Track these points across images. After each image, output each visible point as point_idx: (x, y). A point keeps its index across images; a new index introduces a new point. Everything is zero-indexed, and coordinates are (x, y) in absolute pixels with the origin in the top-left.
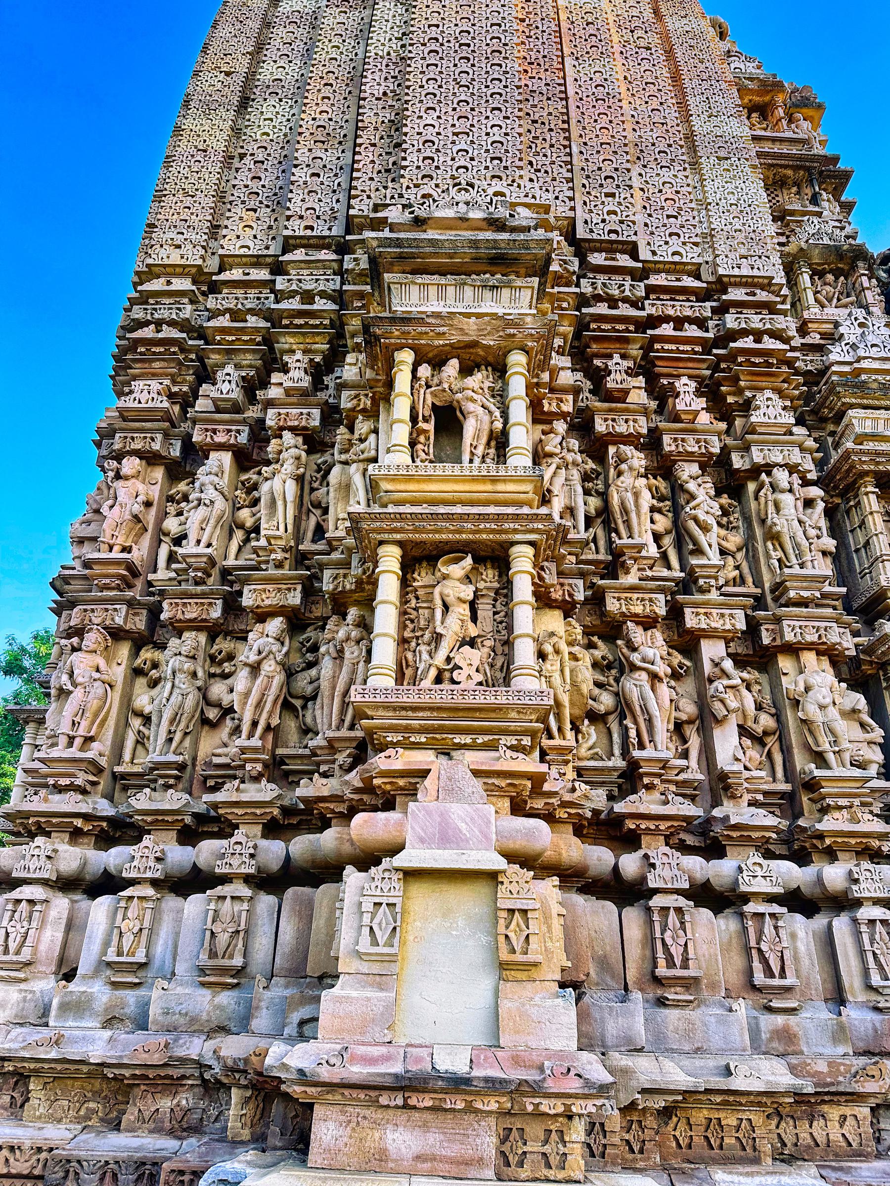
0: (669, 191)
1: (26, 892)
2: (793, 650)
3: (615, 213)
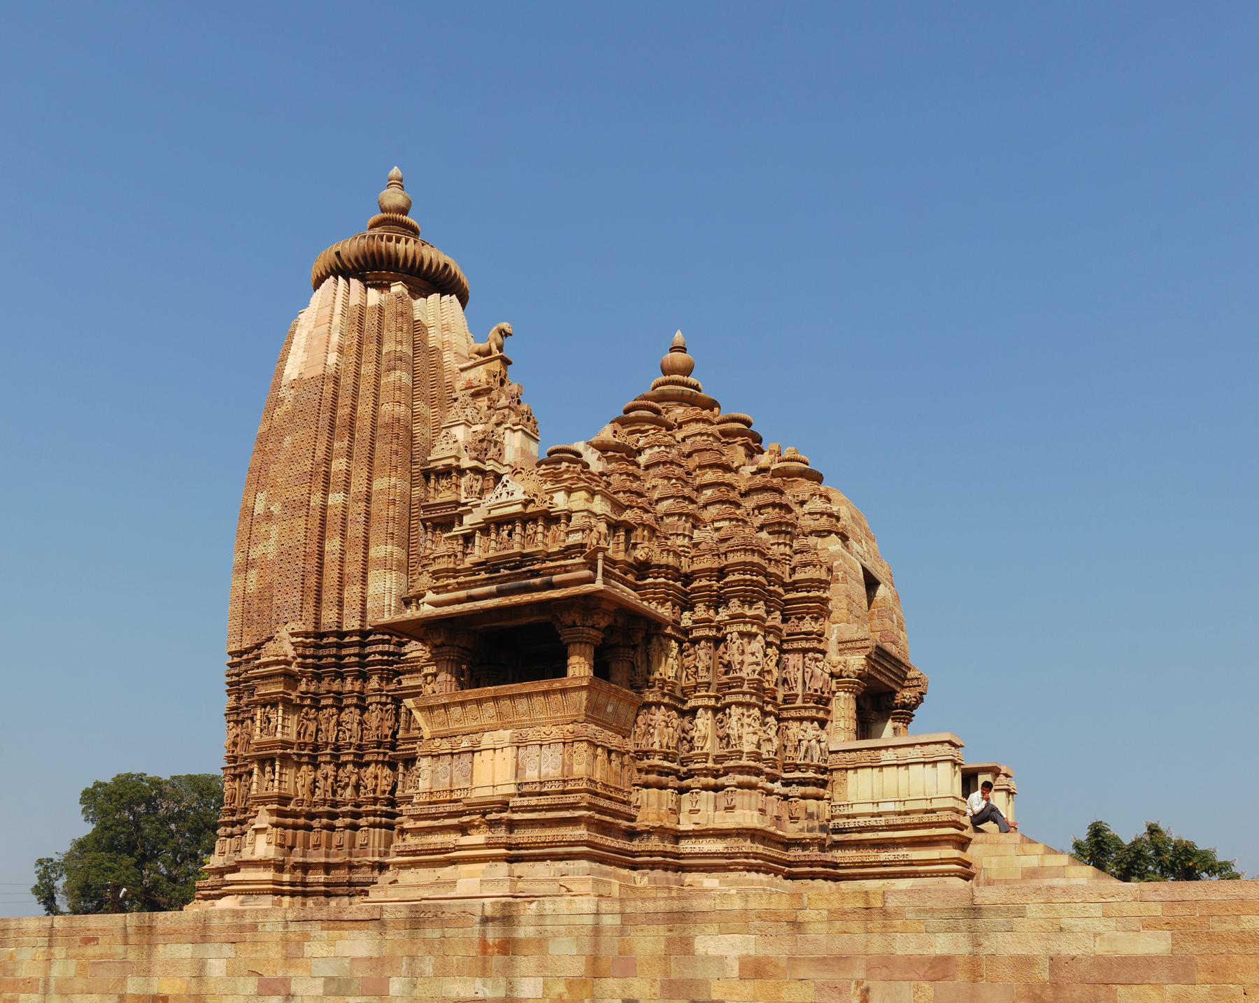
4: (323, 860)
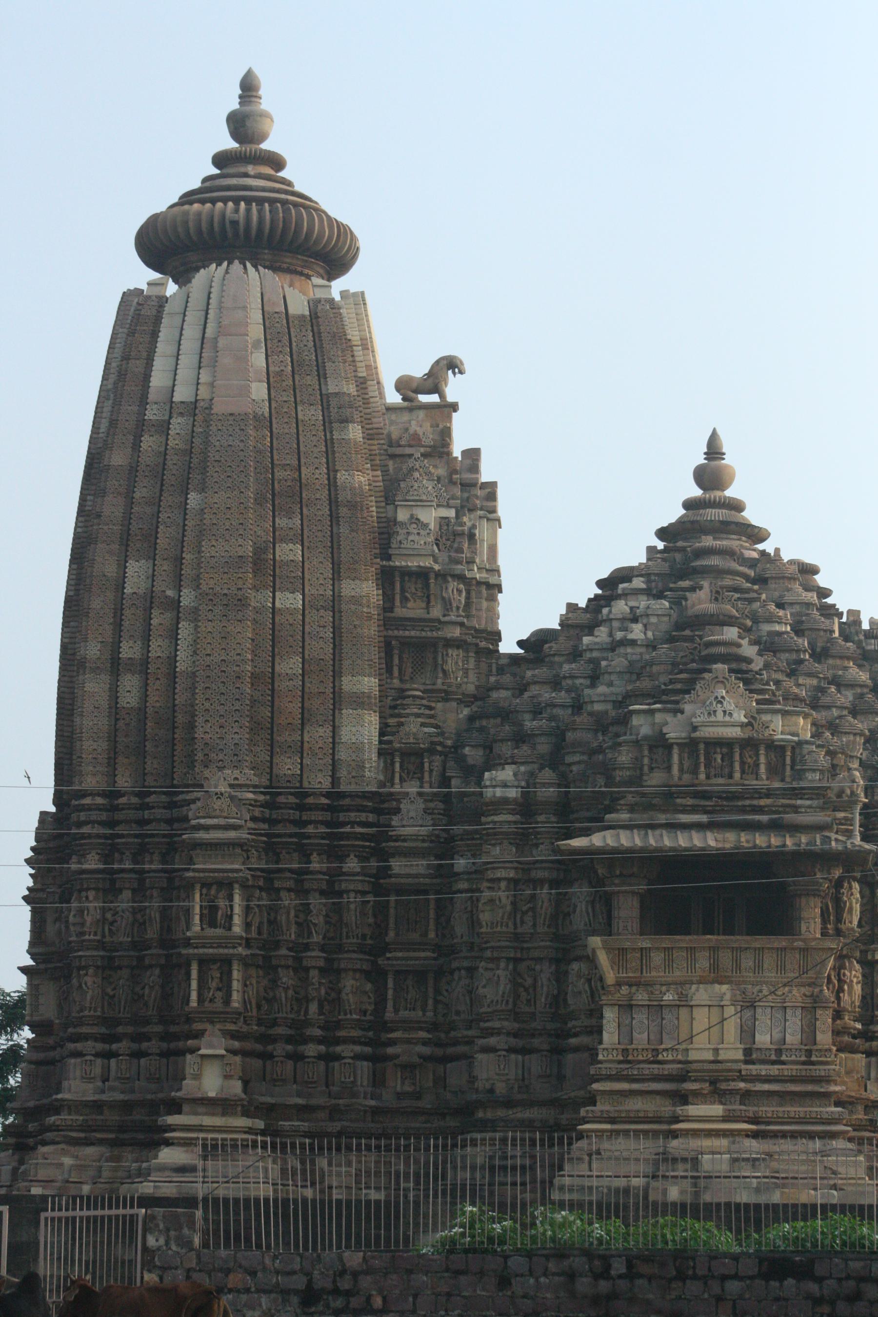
1: (88, 1058)
2: (346, 970)
4: (300, 1101)
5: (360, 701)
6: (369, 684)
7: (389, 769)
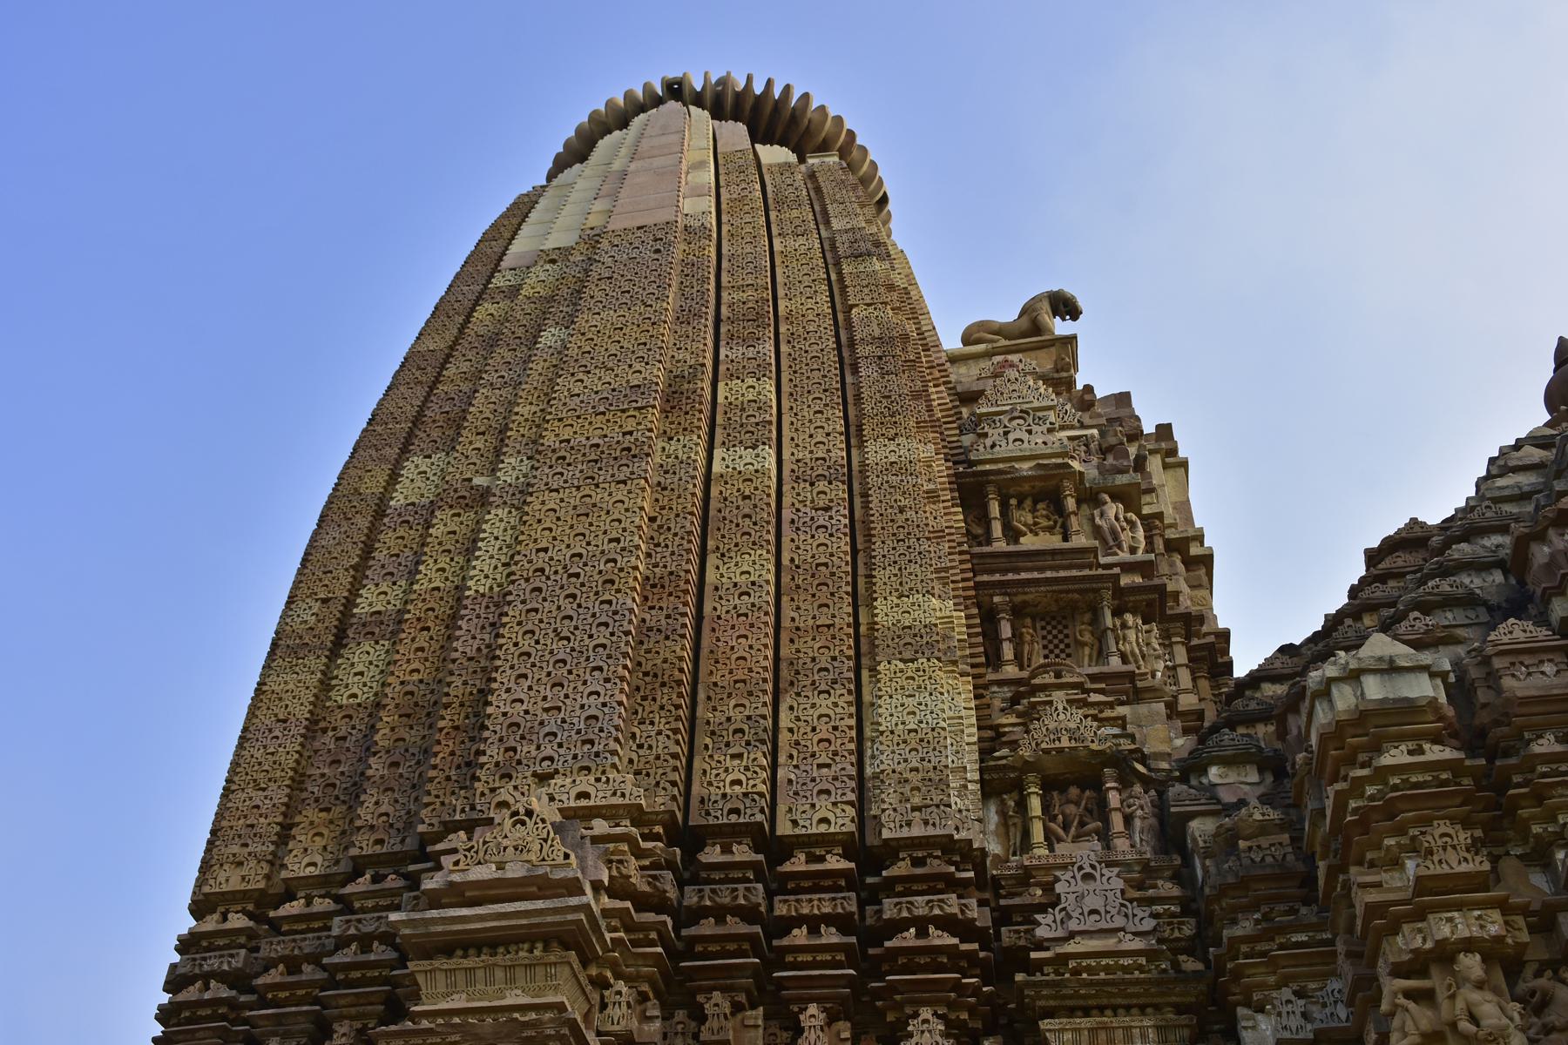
0: (824, 728)
3: (739, 782)
5: (920, 643)
6: (943, 610)
7: (1016, 827)
